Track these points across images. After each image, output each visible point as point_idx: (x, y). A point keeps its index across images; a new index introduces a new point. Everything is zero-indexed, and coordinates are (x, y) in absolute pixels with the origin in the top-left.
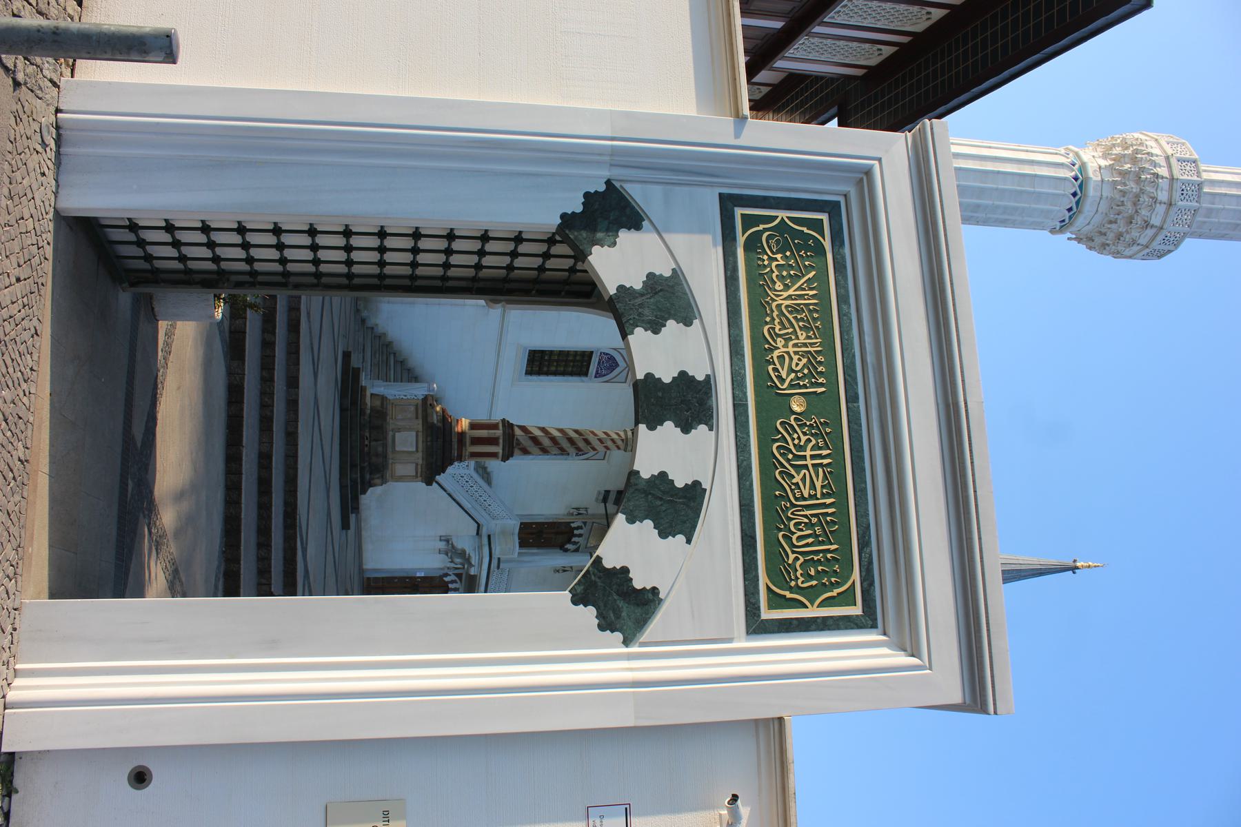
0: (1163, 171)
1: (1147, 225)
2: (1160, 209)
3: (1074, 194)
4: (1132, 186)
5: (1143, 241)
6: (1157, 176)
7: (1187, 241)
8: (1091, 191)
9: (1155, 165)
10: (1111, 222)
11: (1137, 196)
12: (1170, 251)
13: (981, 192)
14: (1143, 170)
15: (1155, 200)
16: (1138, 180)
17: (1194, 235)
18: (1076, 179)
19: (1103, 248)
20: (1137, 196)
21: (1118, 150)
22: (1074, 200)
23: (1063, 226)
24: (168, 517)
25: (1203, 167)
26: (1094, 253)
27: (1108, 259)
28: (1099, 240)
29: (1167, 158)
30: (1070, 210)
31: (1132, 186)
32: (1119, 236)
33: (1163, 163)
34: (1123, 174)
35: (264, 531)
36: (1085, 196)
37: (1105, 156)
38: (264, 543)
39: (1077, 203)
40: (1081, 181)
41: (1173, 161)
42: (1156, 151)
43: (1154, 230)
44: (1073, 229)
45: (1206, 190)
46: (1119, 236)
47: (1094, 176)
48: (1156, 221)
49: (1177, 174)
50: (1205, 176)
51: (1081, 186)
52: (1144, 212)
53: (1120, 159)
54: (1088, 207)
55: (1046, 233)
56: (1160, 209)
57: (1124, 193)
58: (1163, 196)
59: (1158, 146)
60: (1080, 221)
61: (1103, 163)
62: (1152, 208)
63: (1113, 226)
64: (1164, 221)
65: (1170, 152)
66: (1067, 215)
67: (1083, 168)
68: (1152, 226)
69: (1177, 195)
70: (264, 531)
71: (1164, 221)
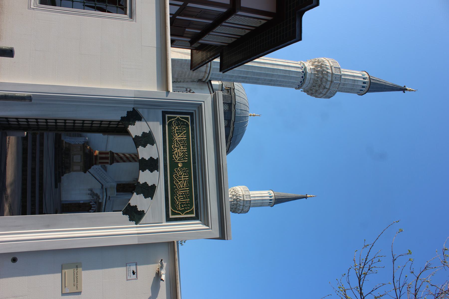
0: (330, 71)
1: (325, 88)
3: (302, 77)
5: (324, 93)
6: (328, 72)
7: (338, 93)
8: (308, 76)
9: (327, 69)
10: (314, 86)
11: (322, 78)
12: (332, 96)
14: (324, 70)
15: (327, 80)
16: (322, 74)
17: (339, 91)
18: (303, 72)
19: (312, 94)
20: (322, 78)
21: (316, 63)
22: (302, 79)
23: (299, 87)
24: (9, 191)
25: (342, 70)
26: (309, 96)
28: (310, 92)
29: (331, 67)
30: (301, 82)
32: (316, 91)
33: (330, 68)
34: (318, 71)
35: (33, 192)
36: (306, 78)
37: (312, 65)
38: (33, 196)
39: (303, 80)
40: (305, 73)
41: (333, 68)
42: (328, 64)
43: (327, 90)
45: (342, 77)
46: (316, 91)
47: (308, 71)
48: (327, 87)
49: (334, 72)
50: (342, 73)
51: (304, 75)
52: (324, 84)
53: (317, 66)
54: (307, 81)
55: (294, 89)
57: (318, 77)
58: (329, 79)
59: (329, 62)
60: (304, 86)
61: (312, 67)
62: (326, 83)
63: (315, 88)
64: (330, 87)
65: (332, 65)
66: (300, 84)
67: (305, 68)
68: (326, 88)
69: (334, 79)
70: (33, 192)
71: (330, 87)
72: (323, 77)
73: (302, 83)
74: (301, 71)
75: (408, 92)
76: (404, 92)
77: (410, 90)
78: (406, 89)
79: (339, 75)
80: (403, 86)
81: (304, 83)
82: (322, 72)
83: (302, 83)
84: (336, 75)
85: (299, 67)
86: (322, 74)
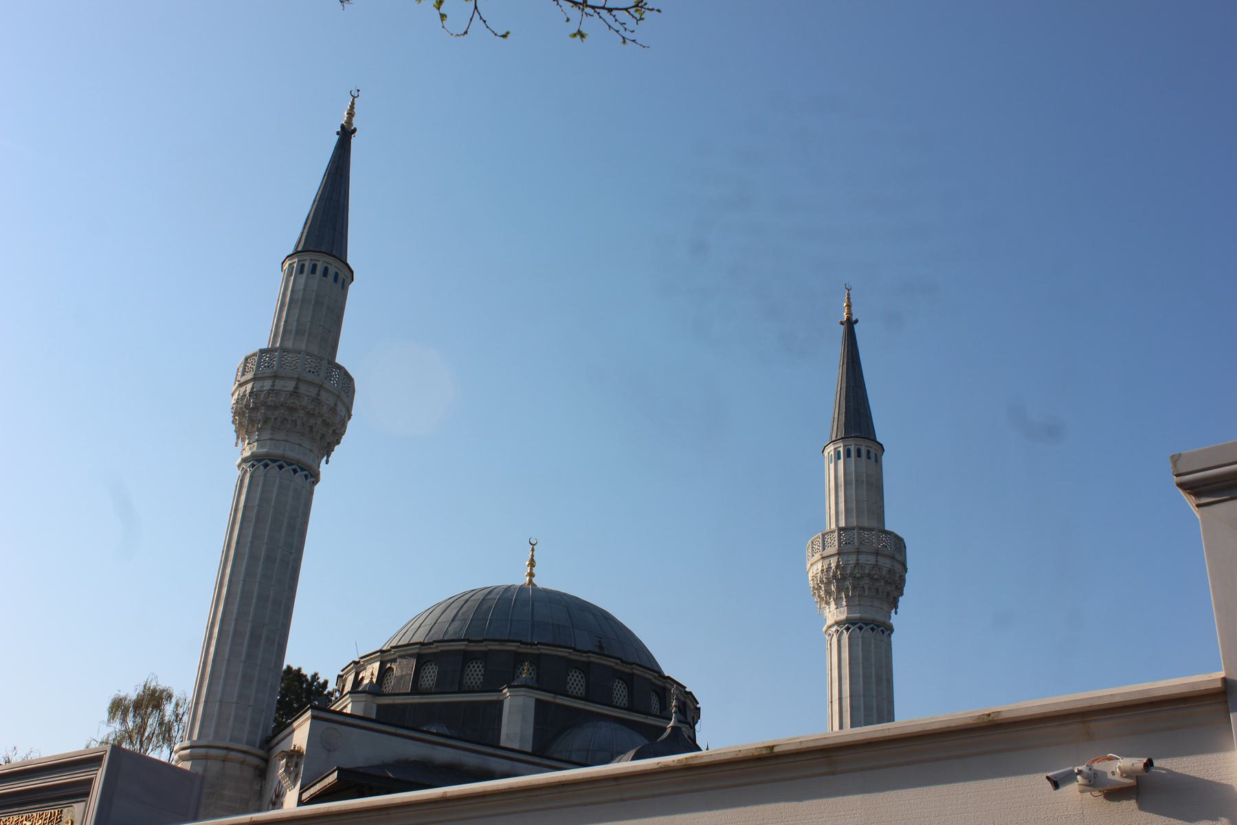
0: (833, 562)
2: (863, 559)
4: (848, 583)
6: (837, 567)
9: (829, 567)
13: (867, 708)
14: (835, 576)
18: (848, 629)
25: (828, 529)
30: (873, 629)
31: (848, 583)
33: (827, 561)
34: (839, 590)
36: (861, 619)
37: (828, 603)
40: (848, 624)
41: (826, 553)
42: (819, 565)
45: (842, 524)
50: (833, 526)
53: (828, 593)
54: (869, 615)
56: (863, 559)
57: (854, 588)
58: (852, 560)
59: (815, 568)
61: (833, 604)
65: (817, 556)
67: (838, 623)
72: (852, 575)
74: (846, 635)
75: (853, 311)
76: (856, 321)
77: (849, 306)
78: (848, 319)
79: (839, 535)
80: (842, 327)
81: (873, 621)
82: (838, 581)
85: (839, 641)
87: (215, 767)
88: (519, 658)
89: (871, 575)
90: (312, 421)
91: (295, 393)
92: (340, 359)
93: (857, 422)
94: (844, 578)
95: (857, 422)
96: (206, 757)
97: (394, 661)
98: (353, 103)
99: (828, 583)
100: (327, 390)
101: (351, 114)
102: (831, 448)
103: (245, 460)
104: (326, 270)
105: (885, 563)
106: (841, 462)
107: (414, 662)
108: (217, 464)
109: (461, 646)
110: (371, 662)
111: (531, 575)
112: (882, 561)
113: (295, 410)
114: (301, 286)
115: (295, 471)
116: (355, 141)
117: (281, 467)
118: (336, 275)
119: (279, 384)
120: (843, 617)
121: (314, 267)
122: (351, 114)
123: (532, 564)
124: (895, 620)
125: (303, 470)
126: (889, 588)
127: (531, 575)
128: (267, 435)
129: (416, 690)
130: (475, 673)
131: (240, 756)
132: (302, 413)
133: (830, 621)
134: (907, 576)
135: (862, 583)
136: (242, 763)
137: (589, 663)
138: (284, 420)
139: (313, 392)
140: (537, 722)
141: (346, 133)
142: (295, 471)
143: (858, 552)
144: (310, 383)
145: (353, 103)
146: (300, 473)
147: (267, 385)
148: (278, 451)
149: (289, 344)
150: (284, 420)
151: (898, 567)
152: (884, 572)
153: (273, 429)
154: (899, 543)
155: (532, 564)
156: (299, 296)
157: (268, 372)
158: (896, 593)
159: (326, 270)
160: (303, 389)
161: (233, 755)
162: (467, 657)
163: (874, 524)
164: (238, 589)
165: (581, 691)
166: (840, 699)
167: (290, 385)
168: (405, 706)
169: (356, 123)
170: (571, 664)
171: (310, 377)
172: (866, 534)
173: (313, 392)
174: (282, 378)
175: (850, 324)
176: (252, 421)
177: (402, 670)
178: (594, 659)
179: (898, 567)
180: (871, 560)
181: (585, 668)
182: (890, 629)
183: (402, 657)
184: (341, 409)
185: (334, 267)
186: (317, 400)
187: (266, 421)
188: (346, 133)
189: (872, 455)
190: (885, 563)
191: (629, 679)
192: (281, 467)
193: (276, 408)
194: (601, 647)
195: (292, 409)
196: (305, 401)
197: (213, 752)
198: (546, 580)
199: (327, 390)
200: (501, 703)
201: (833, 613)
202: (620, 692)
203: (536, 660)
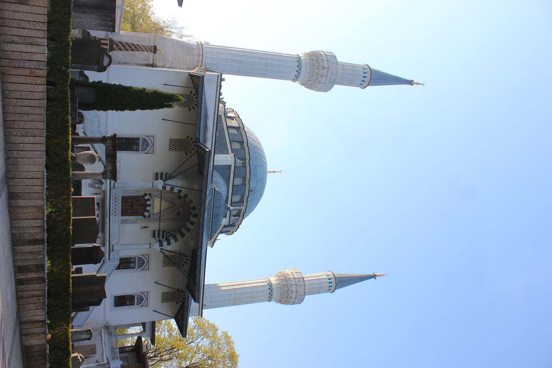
0: (291, 276)
2: (294, 286)
8: (274, 287)
14: (286, 277)
27: (289, 306)
34: (282, 280)
40: (270, 285)
41: (294, 274)
44: (273, 299)
45: (305, 279)
49: (295, 276)
53: (280, 276)
54: (274, 291)
56: (294, 286)
57: (283, 285)
58: (293, 283)
60: (274, 295)
65: (292, 271)
67: (270, 281)
72: (288, 283)
73: (271, 294)
74: (266, 284)
77: (380, 275)
78: (376, 275)
83: (271, 294)
84: (298, 278)
86: (286, 281)
87: (196, 52)
88: (244, 159)
89: (288, 291)
90: (315, 75)
91: (324, 68)
92: (336, 87)
93: (341, 282)
94: (286, 281)
95: (341, 282)
96: (199, 49)
97: (236, 120)
98: (420, 84)
99: (283, 276)
100: (326, 79)
101: (417, 84)
102: (330, 273)
103: (298, 55)
104: (366, 77)
105: (294, 295)
106: (326, 277)
107: (237, 126)
108: (296, 46)
109: (245, 140)
110: (234, 114)
111: (270, 172)
112: (294, 293)
113: (317, 71)
114: (358, 69)
115: (297, 71)
116: (408, 86)
117: (298, 66)
118: (364, 81)
119: (326, 62)
120: (272, 282)
121: (366, 73)
122: (417, 84)
123: (274, 172)
124: (273, 303)
125: (298, 74)
126: (285, 298)
127: (270, 172)
128: (308, 61)
129: (228, 127)
130: (237, 146)
131: (201, 60)
132: (317, 71)
133: (270, 279)
134: (289, 306)
135: (286, 287)
136: (199, 61)
137: (245, 185)
138: (313, 66)
139: (325, 74)
140: (223, 166)
141: (411, 83)
142: (297, 71)
143: (296, 285)
144: (328, 73)
145: (420, 84)
146: (295, 78)
147: (325, 59)
148: (303, 64)
149: (339, 66)
150: (313, 66)
151: (293, 300)
152: (291, 295)
153: (310, 63)
154: (301, 301)
155: (274, 172)
156: (355, 69)
157: (329, 59)
158: (283, 301)
159: (366, 77)
160: (325, 70)
161: (201, 57)
162: (241, 143)
163: (307, 291)
164: (255, 55)
165: (235, 184)
166: (243, 284)
167: (326, 66)
168: (222, 124)
169: (415, 85)
170: (244, 179)
171: (330, 73)
172: (303, 287)
173: (325, 74)
174: (328, 63)
175: (374, 276)
176: (312, 56)
177: (234, 123)
178: (247, 187)
179: (293, 300)
180: (294, 290)
181: (244, 184)
182: (269, 301)
183: (238, 123)
184: (320, 86)
185: (367, 80)
186: (322, 76)
187: (313, 60)
188: (411, 83)
189: (330, 288)
190: (294, 295)
191: (241, 201)
192: (298, 66)
193: (318, 62)
194: (251, 191)
195: (318, 68)
196: (321, 72)
197: (201, 50)
198: (269, 176)
199: (326, 79)
200: (228, 154)
201: (273, 280)
202: (237, 198)
203: (244, 166)
